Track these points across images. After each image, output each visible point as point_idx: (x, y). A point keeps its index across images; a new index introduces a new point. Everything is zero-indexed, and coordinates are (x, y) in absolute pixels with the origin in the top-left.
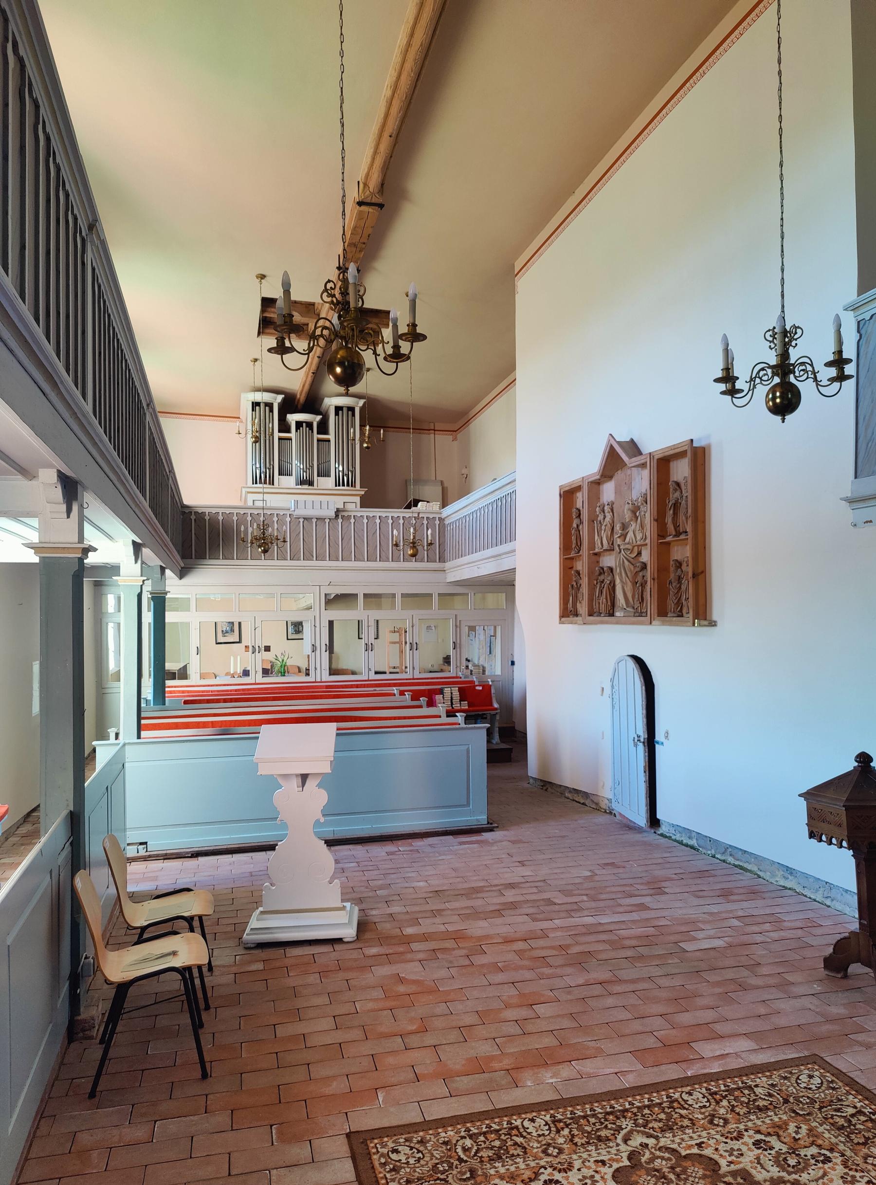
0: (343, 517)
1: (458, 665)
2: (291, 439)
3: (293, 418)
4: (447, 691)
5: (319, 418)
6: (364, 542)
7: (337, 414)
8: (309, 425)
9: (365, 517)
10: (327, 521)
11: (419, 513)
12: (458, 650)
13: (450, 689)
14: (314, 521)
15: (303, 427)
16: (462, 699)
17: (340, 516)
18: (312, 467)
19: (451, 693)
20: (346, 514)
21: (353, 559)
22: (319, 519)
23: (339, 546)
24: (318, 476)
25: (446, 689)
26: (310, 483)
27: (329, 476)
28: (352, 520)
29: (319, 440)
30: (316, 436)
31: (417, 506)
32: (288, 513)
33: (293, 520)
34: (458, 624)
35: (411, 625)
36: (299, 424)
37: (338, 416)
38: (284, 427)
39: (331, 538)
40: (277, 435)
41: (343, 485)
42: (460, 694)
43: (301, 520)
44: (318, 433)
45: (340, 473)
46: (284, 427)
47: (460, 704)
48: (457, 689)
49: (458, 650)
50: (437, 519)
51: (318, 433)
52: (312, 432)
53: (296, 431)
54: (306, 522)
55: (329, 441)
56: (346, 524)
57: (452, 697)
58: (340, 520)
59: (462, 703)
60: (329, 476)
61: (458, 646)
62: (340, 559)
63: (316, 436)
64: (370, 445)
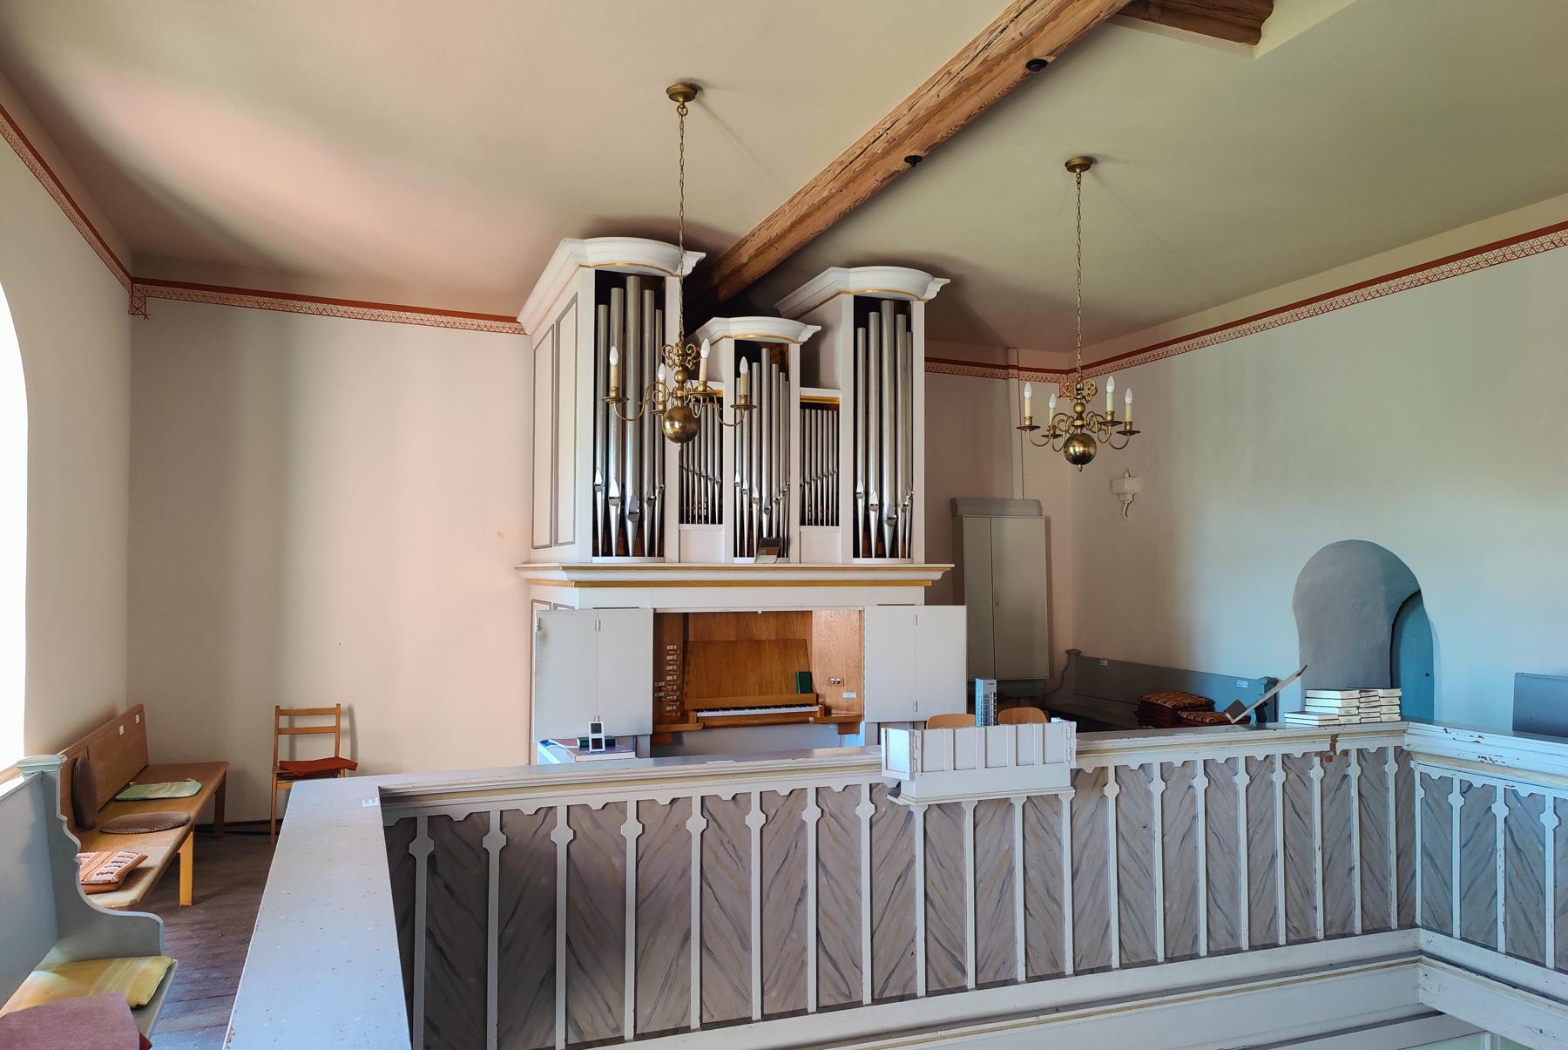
2: (720, 401)
8: (779, 352)
18: (787, 494)
23: (1060, 907)
24: (803, 523)
26: (778, 546)
29: (806, 405)
30: (798, 392)
32: (864, 780)
39: (1032, 873)
41: (880, 554)
44: (803, 384)
51: (803, 384)
52: (787, 378)
63: (798, 392)
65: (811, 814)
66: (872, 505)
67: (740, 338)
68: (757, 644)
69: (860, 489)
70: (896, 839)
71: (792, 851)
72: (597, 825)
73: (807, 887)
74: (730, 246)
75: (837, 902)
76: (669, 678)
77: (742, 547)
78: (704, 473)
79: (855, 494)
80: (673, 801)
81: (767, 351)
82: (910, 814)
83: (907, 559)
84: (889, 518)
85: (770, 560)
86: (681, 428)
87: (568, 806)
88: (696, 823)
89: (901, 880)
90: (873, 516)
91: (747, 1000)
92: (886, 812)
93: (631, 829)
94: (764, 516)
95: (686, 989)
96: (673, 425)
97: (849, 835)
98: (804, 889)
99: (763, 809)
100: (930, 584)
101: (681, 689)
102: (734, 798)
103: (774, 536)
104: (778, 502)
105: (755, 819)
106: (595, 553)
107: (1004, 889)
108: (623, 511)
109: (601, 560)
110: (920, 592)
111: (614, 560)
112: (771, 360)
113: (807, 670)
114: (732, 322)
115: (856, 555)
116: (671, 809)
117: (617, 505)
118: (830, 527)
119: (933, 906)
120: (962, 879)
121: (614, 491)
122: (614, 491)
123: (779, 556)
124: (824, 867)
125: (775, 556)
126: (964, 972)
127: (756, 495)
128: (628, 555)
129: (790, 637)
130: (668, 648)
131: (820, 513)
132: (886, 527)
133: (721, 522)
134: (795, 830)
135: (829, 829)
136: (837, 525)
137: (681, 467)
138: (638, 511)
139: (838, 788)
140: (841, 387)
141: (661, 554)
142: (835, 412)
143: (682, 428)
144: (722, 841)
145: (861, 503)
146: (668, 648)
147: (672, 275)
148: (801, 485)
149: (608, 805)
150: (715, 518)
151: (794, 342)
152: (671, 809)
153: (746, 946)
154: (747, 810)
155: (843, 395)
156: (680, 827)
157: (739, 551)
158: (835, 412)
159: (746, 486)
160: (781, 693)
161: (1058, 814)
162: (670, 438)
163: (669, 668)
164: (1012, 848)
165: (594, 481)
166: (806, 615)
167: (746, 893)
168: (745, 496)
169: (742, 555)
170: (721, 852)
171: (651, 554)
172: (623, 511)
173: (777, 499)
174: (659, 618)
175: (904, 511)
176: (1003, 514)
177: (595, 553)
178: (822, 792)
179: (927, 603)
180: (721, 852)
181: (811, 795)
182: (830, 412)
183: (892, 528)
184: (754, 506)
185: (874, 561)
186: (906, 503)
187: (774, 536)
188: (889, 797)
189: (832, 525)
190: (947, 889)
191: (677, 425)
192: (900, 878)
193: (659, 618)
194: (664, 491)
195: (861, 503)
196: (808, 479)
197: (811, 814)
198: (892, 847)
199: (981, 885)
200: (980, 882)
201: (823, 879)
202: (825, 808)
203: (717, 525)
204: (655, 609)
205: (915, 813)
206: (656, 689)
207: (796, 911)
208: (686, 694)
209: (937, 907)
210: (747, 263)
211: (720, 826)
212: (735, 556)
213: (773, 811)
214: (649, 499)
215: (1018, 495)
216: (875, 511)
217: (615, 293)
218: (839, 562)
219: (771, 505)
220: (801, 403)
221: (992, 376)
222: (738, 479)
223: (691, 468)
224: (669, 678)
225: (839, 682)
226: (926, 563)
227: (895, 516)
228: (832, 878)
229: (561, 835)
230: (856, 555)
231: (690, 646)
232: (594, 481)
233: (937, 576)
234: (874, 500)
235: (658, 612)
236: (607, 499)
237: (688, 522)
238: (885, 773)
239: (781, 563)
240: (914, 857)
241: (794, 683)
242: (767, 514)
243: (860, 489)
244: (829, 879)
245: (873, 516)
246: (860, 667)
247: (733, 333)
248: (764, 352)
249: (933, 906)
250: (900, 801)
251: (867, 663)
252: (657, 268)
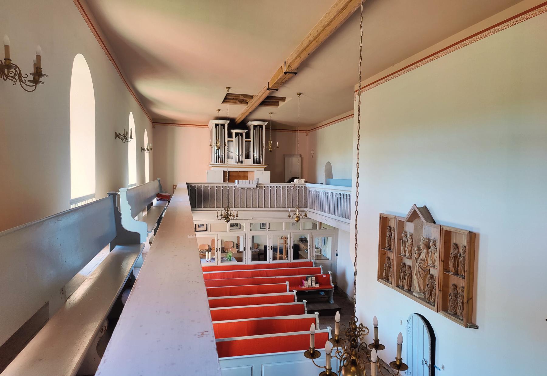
0: (259, 187)
1: (312, 256)
2: (233, 141)
3: (234, 131)
4: (310, 279)
5: (246, 131)
6: (269, 198)
7: (254, 129)
8: (241, 134)
9: (270, 187)
10: (252, 189)
11: (295, 185)
12: (312, 249)
13: (311, 278)
14: (246, 189)
15: (238, 136)
16: (316, 283)
17: (258, 187)
19: (312, 280)
20: (261, 186)
21: (264, 207)
22: (248, 188)
24: (245, 158)
25: (309, 278)
26: (242, 162)
27: (250, 158)
28: (264, 189)
29: (246, 141)
31: (294, 181)
33: (236, 188)
34: (312, 236)
35: (290, 237)
36: (237, 134)
38: (230, 135)
39: (254, 197)
40: (226, 139)
41: (257, 163)
42: (316, 280)
43: (240, 189)
44: (245, 138)
45: (256, 157)
46: (230, 135)
47: (316, 285)
48: (314, 278)
49: (312, 249)
50: (303, 187)
51: (245, 138)
52: (243, 138)
53: (235, 137)
54: (242, 189)
55: (250, 142)
56: (261, 190)
57: (312, 282)
58: (258, 189)
59: (317, 284)
60: (250, 158)
61: (312, 247)
62: (258, 207)
63: (244, 139)
64: (272, 150)
69: (254, 154)
77: (237, 162)
85: (239, 164)
88: (216, 188)
91: (221, 206)
93: (209, 188)
95: (215, 204)
104: (241, 156)
105: (222, 188)
109: (216, 164)
110: (264, 169)
111: (217, 164)
112: (240, 135)
115: (253, 163)
126: (245, 206)
131: (248, 157)
137: (227, 151)
141: (224, 163)
150: (232, 158)
153: (221, 201)
155: (252, 140)
159: (236, 153)
161: (257, 191)
164: (251, 193)
174: (224, 172)
179: (265, 170)
185: (256, 164)
193: (224, 172)
195: (254, 156)
217: (218, 127)
218: (251, 164)
221: (293, 132)
229: (202, 188)
230: (253, 163)
233: (266, 166)
234: (256, 155)
236: (216, 155)
243: (254, 154)
248: (239, 134)
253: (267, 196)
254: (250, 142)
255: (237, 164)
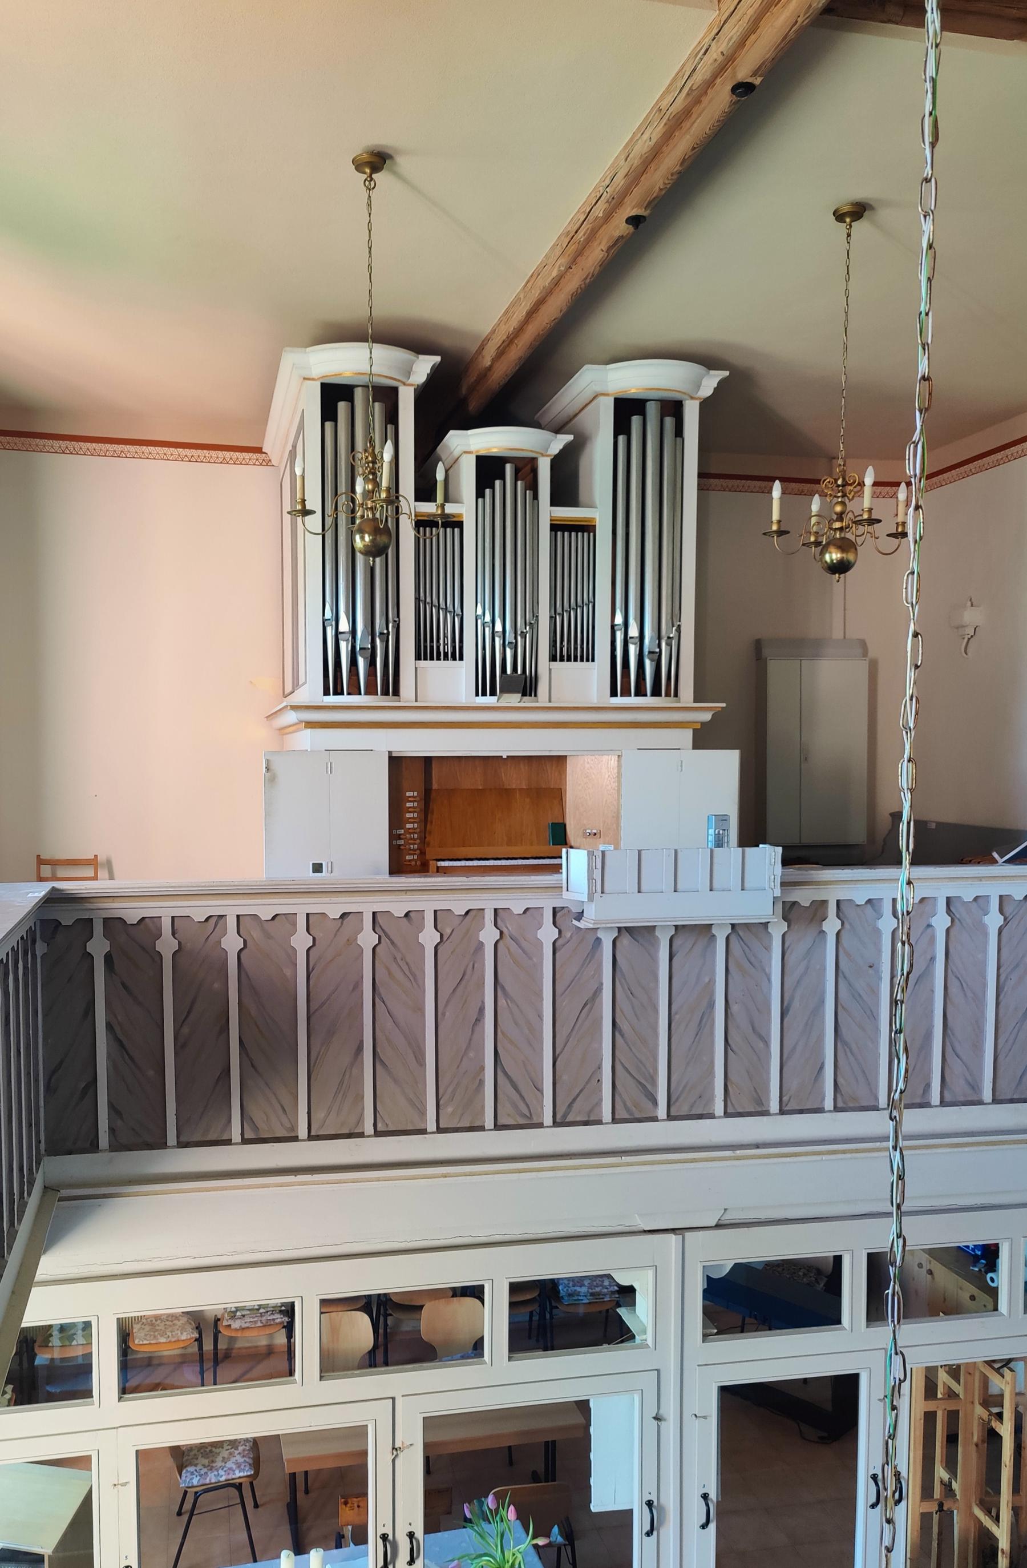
2: (460, 525)
7: (621, 427)
15: (503, 477)
18: (534, 626)
23: (767, 1044)
24: (553, 658)
26: (528, 686)
28: (832, 925)
32: (547, 904)
33: (568, 934)
37: (628, 434)
39: (734, 1008)
40: (410, 505)
41: (640, 692)
44: (553, 503)
51: (553, 503)
52: (535, 497)
53: (480, 494)
54: (626, 940)
63: (548, 512)
65: (488, 935)
66: (631, 638)
67: (483, 453)
68: (505, 793)
69: (619, 619)
70: (583, 965)
71: (469, 972)
72: (268, 936)
73: (484, 1008)
74: (474, 348)
75: (516, 1024)
76: (408, 826)
78: (442, 605)
79: (613, 627)
80: (344, 916)
81: (511, 468)
82: (598, 940)
83: (672, 698)
84: (650, 652)
85: (513, 699)
86: (371, 541)
87: (238, 916)
88: (367, 939)
89: (588, 1007)
90: (633, 650)
92: (571, 936)
93: (301, 941)
94: (509, 653)
96: (362, 538)
97: (530, 958)
98: (482, 1010)
99: (438, 927)
100: (699, 726)
101: (423, 840)
102: (407, 915)
103: (519, 672)
105: (429, 937)
106: (326, 693)
107: (704, 1020)
108: (353, 647)
109: (332, 699)
110: (687, 736)
113: (561, 821)
114: (471, 435)
116: (342, 923)
117: (347, 640)
118: (585, 663)
119: (622, 1036)
120: (656, 1009)
121: (344, 626)
122: (344, 626)
123: (524, 694)
124: (503, 989)
125: (520, 695)
127: (498, 627)
128: (360, 694)
129: (544, 786)
130: (408, 794)
132: (648, 663)
133: (461, 658)
134: (472, 951)
135: (509, 950)
136: (593, 660)
137: (417, 599)
138: (369, 646)
139: (518, 910)
140: (598, 506)
141: (396, 692)
142: (592, 534)
143: (372, 541)
144: (395, 958)
145: (619, 636)
146: (408, 794)
147: (404, 384)
148: (551, 617)
149: (278, 917)
151: (543, 455)
152: (342, 923)
154: (421, 927)
156: (351, 941)
157: (481, 690)
158: (592, 534)
159: (488, 618)
160: (532, 845)
162: (361, 552)
163: (408, 815)
164: (712, 982)
165: (324, 615)
166: (560, 761)
167: (421, 1010)
168: (487, 630)
169: (484, 694)
170: (394, 968)
171: (385, 692)
172: (353, 647)
173: (522, 632)
174: (396, 763)
175: (669, 645)
176: (816, 655)
177: (326, 693)
178: (501, 913)
180: (394, 968)
181: (489, 916)
182: (586, 534)
183: (654, 663)
184: (497, 639)
185: (633, 700)
186: (671, 636)
187: (519, 672)
188: (575, 922)
189: (588, 660)
190: (638, 1019)
191: (367, 538)
192: (586, 1004)
193: (396, 763)
194: (399, 625)
195: (619, 636)
196: (559, 610)
197: (488, 935)
198: (578, 973)
199: (677, 1017)
200: (676, 1013)
201: (502, 1002)
202: (505, 930)
203: (458, 662)
204: (390, 753)
205: (603, 939)
206: (393, 837)
207: (473, 1031)
208: (428, 844)
209: (626, 1035)
210: (491, 367)
211: (393, 943)
212: (477, 695)
213: (448, 931)
214: (381, 634)
215: (837, 634)
216: (635, 644)
217: (342, 407)
218: (594, 701)
219: (516, 638)
220: (551, 525)
222: (480, 611)
223: (428, 600)
224: (408, 826)
225: (595, 834)
226: (694, 702)
227: (658, 650)
228: (513, 1001)
231: (433, 795)
232: (324, 615)
233: (707, 717)
234: (634, 631)
235: (394, 755)
237: (425, 659)
238: (565, 895)
239: (528, 702)
240: (602, 984)
241: (547, 834)
242: (511, 649)
244: (509, 1002)
245: (633, 650)
246: (617, 817)
247: (473, 448)
248: (508, 467)
249: (622, 1036)
250: (581, 925)
251: (622, 813)
252: (386, 377)
253: (857, 996)
254: (587, 528)
255: (489, 700)
